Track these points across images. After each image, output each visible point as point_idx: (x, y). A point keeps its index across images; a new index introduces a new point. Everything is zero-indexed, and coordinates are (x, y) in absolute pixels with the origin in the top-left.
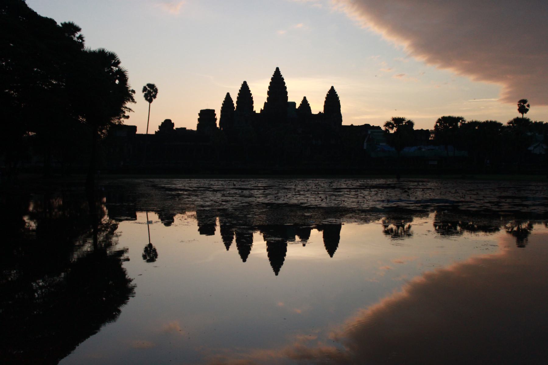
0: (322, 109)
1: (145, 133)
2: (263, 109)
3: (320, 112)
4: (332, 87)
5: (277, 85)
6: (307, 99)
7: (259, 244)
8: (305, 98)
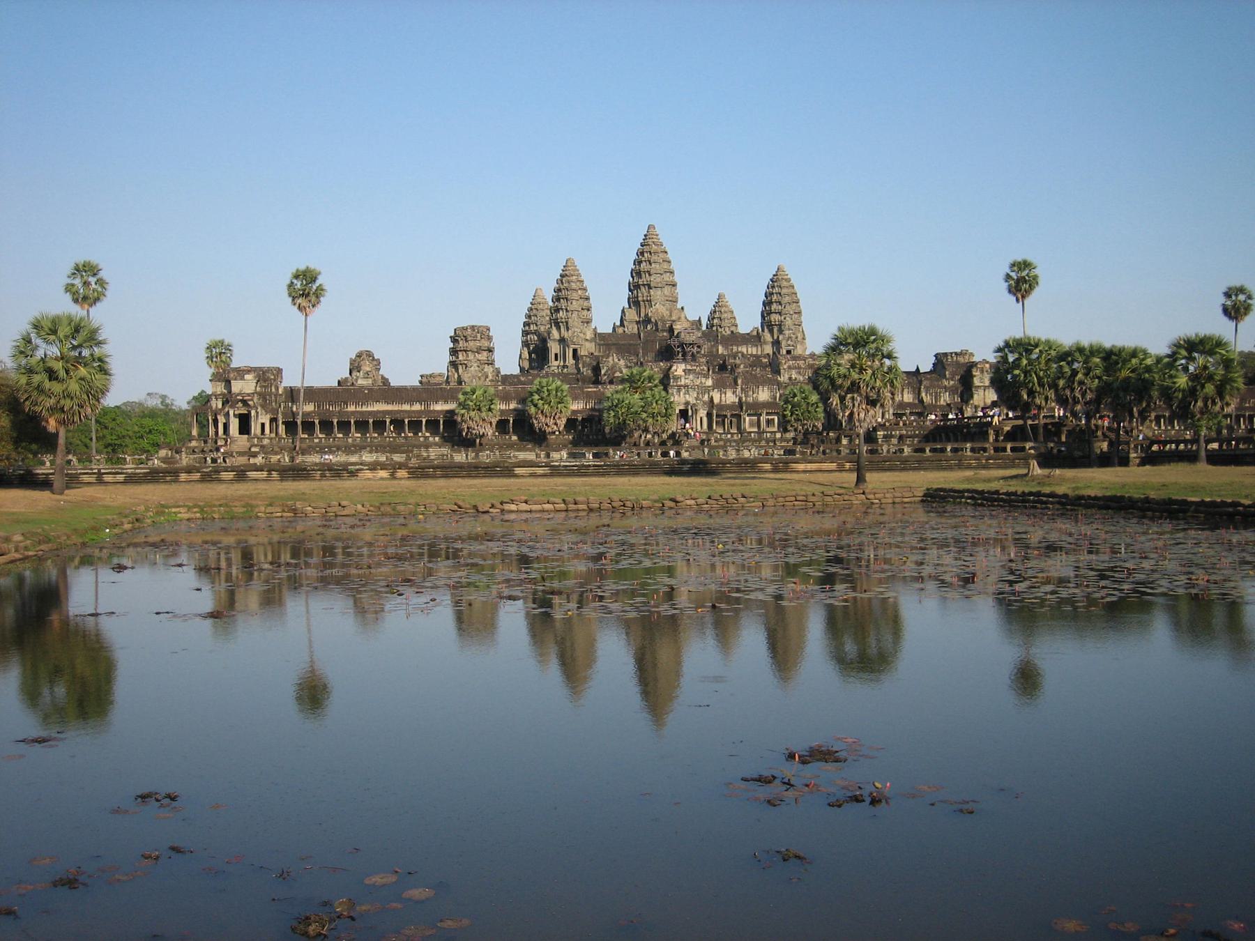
0: (757, 322)
1: (299, 385)
2: (618, 323)
8: (720, 297)
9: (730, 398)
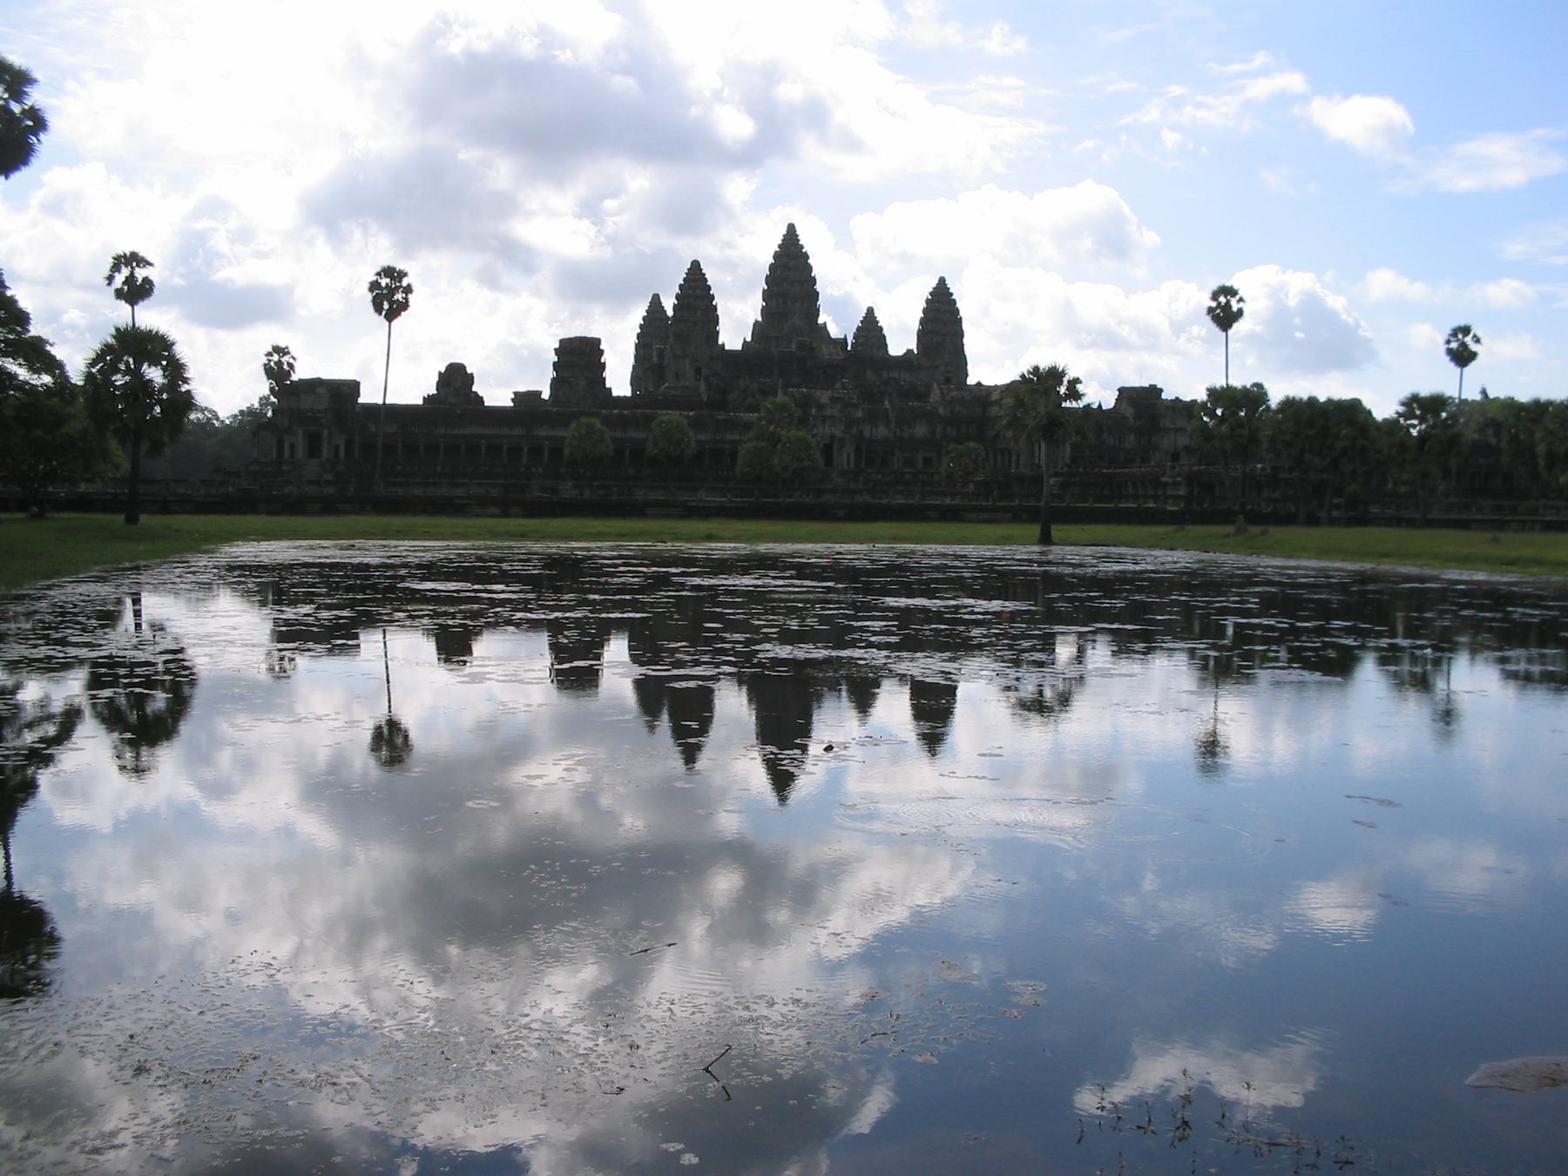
0: (911, 344)
3: (909, 352)
4: (942, 281)
5: (790, 275)
6: (877, 314)
9: (882, 432)
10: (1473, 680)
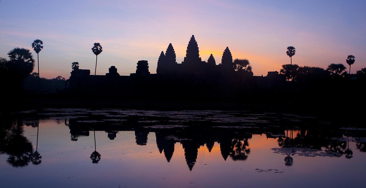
2: (183, 61)
3: (220, 64)
4: (227, 47)
7: (179, 149)
10: (262, 146)
